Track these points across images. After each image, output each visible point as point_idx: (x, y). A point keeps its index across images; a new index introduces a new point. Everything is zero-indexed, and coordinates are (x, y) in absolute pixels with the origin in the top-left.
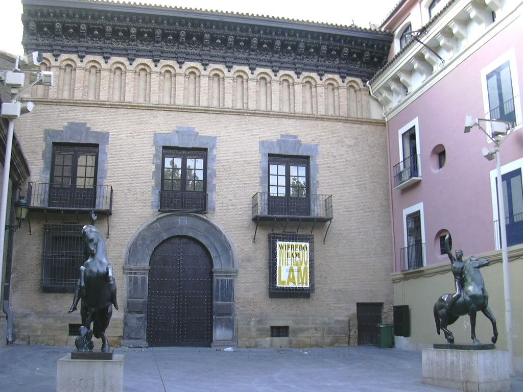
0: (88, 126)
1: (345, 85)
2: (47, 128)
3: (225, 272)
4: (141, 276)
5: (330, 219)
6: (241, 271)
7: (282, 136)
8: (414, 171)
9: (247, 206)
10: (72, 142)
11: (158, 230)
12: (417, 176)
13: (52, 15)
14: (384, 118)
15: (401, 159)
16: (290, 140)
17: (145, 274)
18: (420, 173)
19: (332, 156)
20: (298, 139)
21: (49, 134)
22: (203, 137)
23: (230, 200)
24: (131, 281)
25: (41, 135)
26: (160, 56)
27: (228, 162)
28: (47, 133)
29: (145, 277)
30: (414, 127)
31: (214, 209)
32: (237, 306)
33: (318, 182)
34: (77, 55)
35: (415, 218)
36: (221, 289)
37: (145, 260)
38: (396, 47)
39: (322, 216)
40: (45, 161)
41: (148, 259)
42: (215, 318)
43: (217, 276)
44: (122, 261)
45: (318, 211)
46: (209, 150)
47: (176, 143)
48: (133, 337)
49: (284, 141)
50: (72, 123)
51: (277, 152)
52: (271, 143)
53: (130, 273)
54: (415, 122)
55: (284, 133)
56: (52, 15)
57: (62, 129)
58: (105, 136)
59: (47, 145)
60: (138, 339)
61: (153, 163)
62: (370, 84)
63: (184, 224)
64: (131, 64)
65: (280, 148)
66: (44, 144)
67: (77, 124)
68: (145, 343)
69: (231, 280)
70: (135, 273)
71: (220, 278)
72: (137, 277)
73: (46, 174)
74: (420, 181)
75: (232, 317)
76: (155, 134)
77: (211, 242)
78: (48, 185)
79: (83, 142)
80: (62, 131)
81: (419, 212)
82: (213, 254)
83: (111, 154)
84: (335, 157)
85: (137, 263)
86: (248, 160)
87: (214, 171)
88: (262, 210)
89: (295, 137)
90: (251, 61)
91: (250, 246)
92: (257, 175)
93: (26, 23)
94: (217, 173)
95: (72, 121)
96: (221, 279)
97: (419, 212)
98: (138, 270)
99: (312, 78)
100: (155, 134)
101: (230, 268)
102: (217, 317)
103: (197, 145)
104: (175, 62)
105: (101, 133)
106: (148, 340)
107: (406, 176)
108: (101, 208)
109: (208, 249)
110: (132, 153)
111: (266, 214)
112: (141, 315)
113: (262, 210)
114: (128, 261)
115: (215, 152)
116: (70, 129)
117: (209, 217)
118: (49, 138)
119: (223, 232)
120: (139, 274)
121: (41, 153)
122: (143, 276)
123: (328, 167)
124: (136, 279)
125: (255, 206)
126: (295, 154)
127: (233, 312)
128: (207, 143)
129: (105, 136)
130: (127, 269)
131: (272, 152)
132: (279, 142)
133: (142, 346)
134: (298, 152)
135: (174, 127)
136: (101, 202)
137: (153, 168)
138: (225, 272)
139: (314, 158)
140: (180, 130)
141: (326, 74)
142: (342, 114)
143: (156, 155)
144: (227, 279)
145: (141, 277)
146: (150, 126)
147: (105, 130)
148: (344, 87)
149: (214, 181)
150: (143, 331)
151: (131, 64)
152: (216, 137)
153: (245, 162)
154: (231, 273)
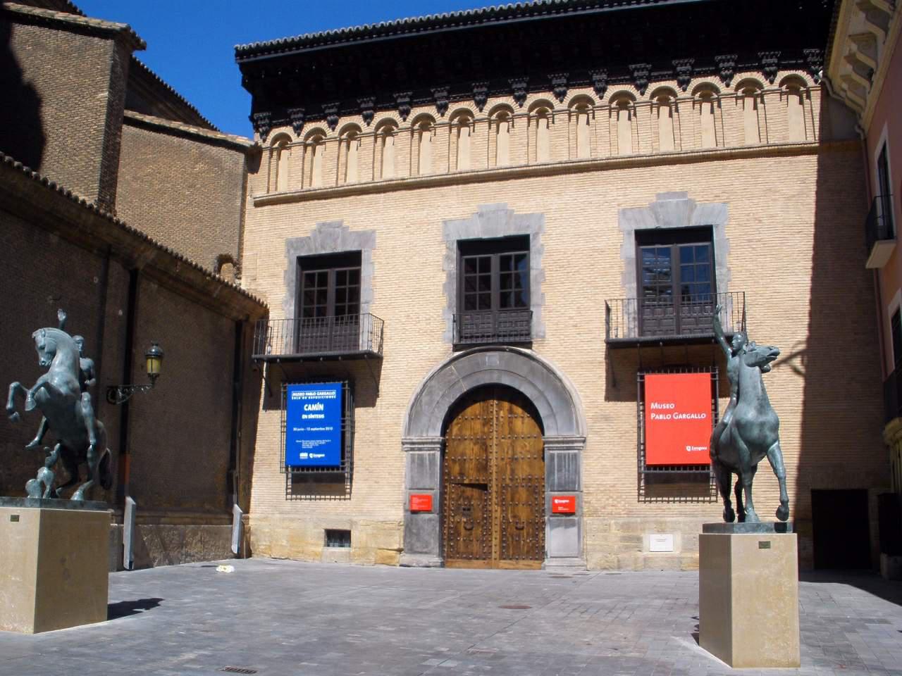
0: (345, 224)
1: (777, 87)
2: (290, 237)
3: (563, 442)
4: (429, 452)
6: (591, 438)
7: (658, 195)
10: (323, 252)
11: (453, 377)
16: (674, 201)
17: (433, 449)
19: (756, 219)
20: (689, 197)
21: (293, 247)
22: (521, 217)
23: (571, 318)
24: (413, 461)
25: (282, 247)
26: (447, 98)
27: (565, 253)
28: (291, 244)
29: (434, 455)
31: (543, 337)
32: (586, 498)
33: (729, 270)
34: (361, 117)
36: (558, 471)
37: (434, 429)
40: (288, 285)
41: (439, 425)
42: (549, 519)
43: (550, 449)
44: (401, 429)
46: (531, 237)
47: (477, 232)
48: (419, 550)
49: (662, 205)
50: (324, 224)
51: (650, 224)
52: (640, 209)
53: (412, 449)
55: (662, 191)
57: (309, 235)
58: (368, 237)
59: (290, 262)
60: (426, 553)
61: (443, 270)
63: (494, 366)
64: (405, 120)
65: (658, 221)
66: (286, 261)
67: (330, 225)
68: (436, 560)
69: (575, 455)
70: (420, 449)
71: (556, 452)
72: (422, 455)
73: (290, 305)
75: (576, 518)
76: (445, 222)
77: (539, 391)
79: (340, 249)
80: (309, 238)
82: (543, 412)
83: (380, 263)
85: (422, 432)
87: (542, 273)
88: (625, 329)
89: (684, 194)
94: (547, 274)
95: (323, 220)
96: (558, 454)
98: (423, 443)
100: (445, 222)
101: (574, 435)
102: (551, 518)
103: (512, 231)
104: (472, 103)
106: (441, 554)
109: (537, 404)
110: (411, 258)
111: (634, 335)
112: (431, 515)
114: (409, 430)
117: (536, 351)
118: (292, 251)
119: (559, 373)
120: (426, 450)
121: (282, 274)
122: (432, 452)
123: (749, 241)
124: (421, 458)
126: (684, 224)
127: (580, 510)
128: (528, 226)
129: (368, 237)
130: (407, 443)
131: (643, 227)
132: (653, 208)
133: (431, 564)
134: (689, 221)
135: (474, 207)
137: (443, 278)
138: (563, 442)
139: (720, 227)
140: (484, 210)
142: (771, 142)
143: (447, 258)
144: (569, 454)
145: (429, 455)
146: (436, 212)
147: (370, 228)
148: (773, 91)
149: (543, 288)
150: (432, 541)
151: (405, 120)
152: (542, 214)
154: (573, 442)
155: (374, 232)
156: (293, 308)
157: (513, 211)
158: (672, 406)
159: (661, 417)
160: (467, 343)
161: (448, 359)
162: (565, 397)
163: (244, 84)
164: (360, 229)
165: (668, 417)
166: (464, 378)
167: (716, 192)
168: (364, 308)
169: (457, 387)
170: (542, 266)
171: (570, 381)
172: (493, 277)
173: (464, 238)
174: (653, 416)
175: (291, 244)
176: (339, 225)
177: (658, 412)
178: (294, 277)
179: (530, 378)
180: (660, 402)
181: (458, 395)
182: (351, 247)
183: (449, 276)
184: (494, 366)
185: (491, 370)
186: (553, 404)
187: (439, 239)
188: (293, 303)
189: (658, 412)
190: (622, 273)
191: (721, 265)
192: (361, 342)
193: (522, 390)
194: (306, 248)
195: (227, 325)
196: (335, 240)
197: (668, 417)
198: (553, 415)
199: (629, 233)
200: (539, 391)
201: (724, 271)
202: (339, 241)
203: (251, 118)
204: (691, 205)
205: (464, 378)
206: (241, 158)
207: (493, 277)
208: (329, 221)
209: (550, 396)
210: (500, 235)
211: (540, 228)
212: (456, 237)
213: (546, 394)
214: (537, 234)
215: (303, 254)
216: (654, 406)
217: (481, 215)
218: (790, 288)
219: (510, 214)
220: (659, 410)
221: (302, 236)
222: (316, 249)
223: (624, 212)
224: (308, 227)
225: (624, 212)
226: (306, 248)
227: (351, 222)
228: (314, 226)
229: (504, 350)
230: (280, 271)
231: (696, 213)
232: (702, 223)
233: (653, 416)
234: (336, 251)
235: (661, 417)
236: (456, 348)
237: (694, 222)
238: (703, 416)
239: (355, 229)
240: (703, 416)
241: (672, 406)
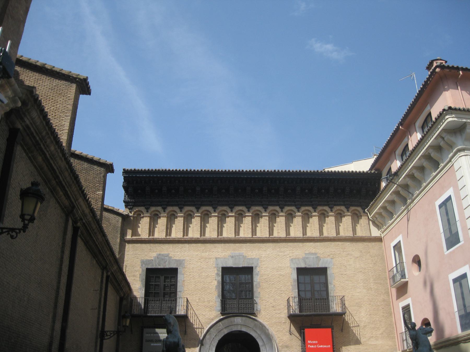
0: (170, 255)
5: (344, 314)
7: (306, 254)
8: (403, 276)
9: (283, 307)
10: (159, 267)
12: (405, 278)
13: (143, 182)
14: (381, 235)
15: (394, 265)
16: (312, 256)
18: (407, 277)
25: (139, 263)
28: (143, 262)
30: (400, 241)
35: (406, 310)
38: (383, 184)
39: (338, 311)
40: (142, 281)
45: (336, 308)
47: (230, 264)
49: (307, 258)
50: (160, 255)
51: (303, 266)
54: (400, 238)
55: (307, 252)
56: (143, 182)
57: (152, 259)
59: (143, 270)
62: (368, 210)
66: (141, 270)
67: (163, 255)
74: (407, 282)
76: (216, 258)
77: (259, 335)
78: (143, 299)
79: (167, 267)
80: (152, 260)
81: (408, 305)
84: (346, 267)
86: (282, 273)
87: (259, 283)
89: (315, 254)
90: (280, 202)
91: (287, 336)
92: (290, 284)
93: (126, 188)
95: (158, 253)
97: (408, 305)
99: (326, 211)
100: (216, 258)
103: (246, 265)
104: (228, 207)
105: (179, 260)
107: (398, 277)
108: (180, 313)
111: (297, 312)
113: (295, 309)
115: (258, 269)
116: (158, 258)
118: (144, 265)
119: (267, 327)
121: (139, 275)
125: (289, 306)
129: (180, 262)
131: (299, 266)
132: (304, 259)
136: (180, 309)
137: (215, 283)
140: (234, 255)
141: (335, 207)
143: (217, 274)
149: (259, 290)
152: (258, 259)
153: (281, 275)
155: (184, 260)
156: (144, 292)
157: (246, 256)
158: (317, 342)
159: (312, 346)
160: (226, 311)
161: (217, 319)
162: (269, 338)
163: (124, 187)
164: (177, 258)
165: (315, 346)
166: (225, 328)
167: (328, 254)
168: (179, 294)
169: (222, 331)
170: (258, 281)
171: (272, 330)
172: (237, 285)
173: (225, 266)
174: (309, 346)
175: (143, 262)
176: (167, 255)
177: (311, 344)
178: (144, 277)
179: (254, 329)
180: (312, 340)
181: (223, 335)
182: (173, 266)
183: (218, 282)
184: (239, 324)
185: (237, 325)
186: (265, 340)
187: (214, 266)
188: (144, 289)
189: (311, 344)
190: (292, 285)
191: (331, 284)
192: (177, 310)
193: (251, 334)
194: (151, 264)
195: (118, 298)
196: (165, 262)
197: (315, 346)
198: (264, 345)
199: (294, 269)
200: (259, 335)
201: (332, 286)
202: (167, 263)
203: (124, 202)
204: (318, 258)
205: (225, 328)
206: (120, 219)
207: (237, 285)
208: (162, 253)
209: (263, 337)
210: (241, 266)
211: (258, 264)
212: (221, 266)
213: (261, 336)
214: (256, 267)
215: (150, 267)
216: (309, 342)
217: (232, 257)
218: (358, 294)
219: (244, 257)
220: (312, 344)
221: (149, 259)
222: (156, 265)
223: (292, 260)
224: (152, 255)
225: (292, 259)
226: (151, 264)
227: (174, 255)
228: (154, 254)
229: (243, 316)
230: (138, 274)
231: (321, 262)
232: (323, 266)
233: (309, 346)
234: (165, 267)
235: (312, 346)
236: (222, 314)
237: (320, 265)
238: (329, 346)
239: (175, 258)
240: (329, 346)
241: (317, 342)
